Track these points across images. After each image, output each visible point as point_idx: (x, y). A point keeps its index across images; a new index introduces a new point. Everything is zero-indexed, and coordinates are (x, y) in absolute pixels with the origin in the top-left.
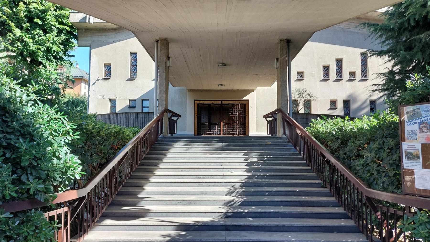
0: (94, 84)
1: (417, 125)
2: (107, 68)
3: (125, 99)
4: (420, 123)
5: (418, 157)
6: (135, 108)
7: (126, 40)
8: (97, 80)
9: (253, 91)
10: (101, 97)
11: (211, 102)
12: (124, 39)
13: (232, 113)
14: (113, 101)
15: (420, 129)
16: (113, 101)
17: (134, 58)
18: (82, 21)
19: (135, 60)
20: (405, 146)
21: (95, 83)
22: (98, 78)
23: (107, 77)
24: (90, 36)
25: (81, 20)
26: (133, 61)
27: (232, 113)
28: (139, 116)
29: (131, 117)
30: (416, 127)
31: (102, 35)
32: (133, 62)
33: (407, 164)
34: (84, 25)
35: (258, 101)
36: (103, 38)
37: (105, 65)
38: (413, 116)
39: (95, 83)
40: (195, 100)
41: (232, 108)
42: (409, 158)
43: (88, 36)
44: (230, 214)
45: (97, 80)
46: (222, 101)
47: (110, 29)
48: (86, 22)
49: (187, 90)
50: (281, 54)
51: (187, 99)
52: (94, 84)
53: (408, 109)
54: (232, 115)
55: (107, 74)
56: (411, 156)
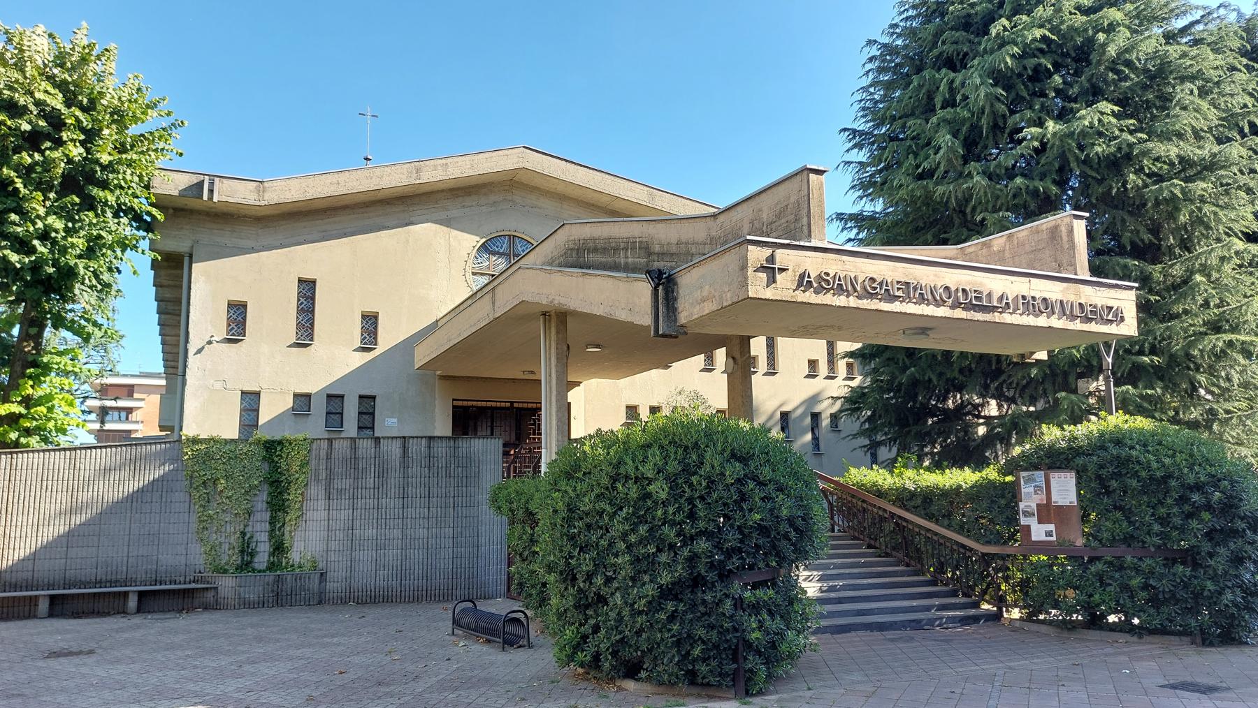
0: (199, 351)
1: (1032, 488)
2: (232, 312)
3: (282, 392)
4: (1035, 487)
5: (1034, 515)
6: (310, 417)
7: (288, 249)
8: (210, 343)
9: (578, 384)
10: (218, 386)
11: (470, 403)
12: (281, 246)
13: (534, 430)
14: (251, 401)
15: (1035, 491)
16: (251, 401)
17: (304, 292)
18: (185, 193)
19: (312, 298)
20: (1022, 505)
21: (203, 348)
22: (212, 336)
23: (233, 335)
24: (188, 227)
25: (185, 190)
26: (302, 300)
27: (534, 430)
28: (434, 444)
29: (413, 446)
30: (1032, 490)
31: (222, 230)
32: (302, 303)
33: (1024, 521)
34: (193, 203)
35: (587, 406)
36: (225, 237)
37: (231, 305)
38: (1028, 481)
39: (203, 348)
40: (454, 400)
41: (534, 420)
42: (1025, 516)
43: (182, 228)
44: (825, 589)
45: (210, 343)
46: (512, 403)
47: (245, 216)
48: (202, 199)
49: (437, 378)
50: (741, 353)
51: (437, 397)
52: (199, 351)
53: (1023, 474)
54: (534, 434)
55: (233, 328)
56: (1028, 514)
